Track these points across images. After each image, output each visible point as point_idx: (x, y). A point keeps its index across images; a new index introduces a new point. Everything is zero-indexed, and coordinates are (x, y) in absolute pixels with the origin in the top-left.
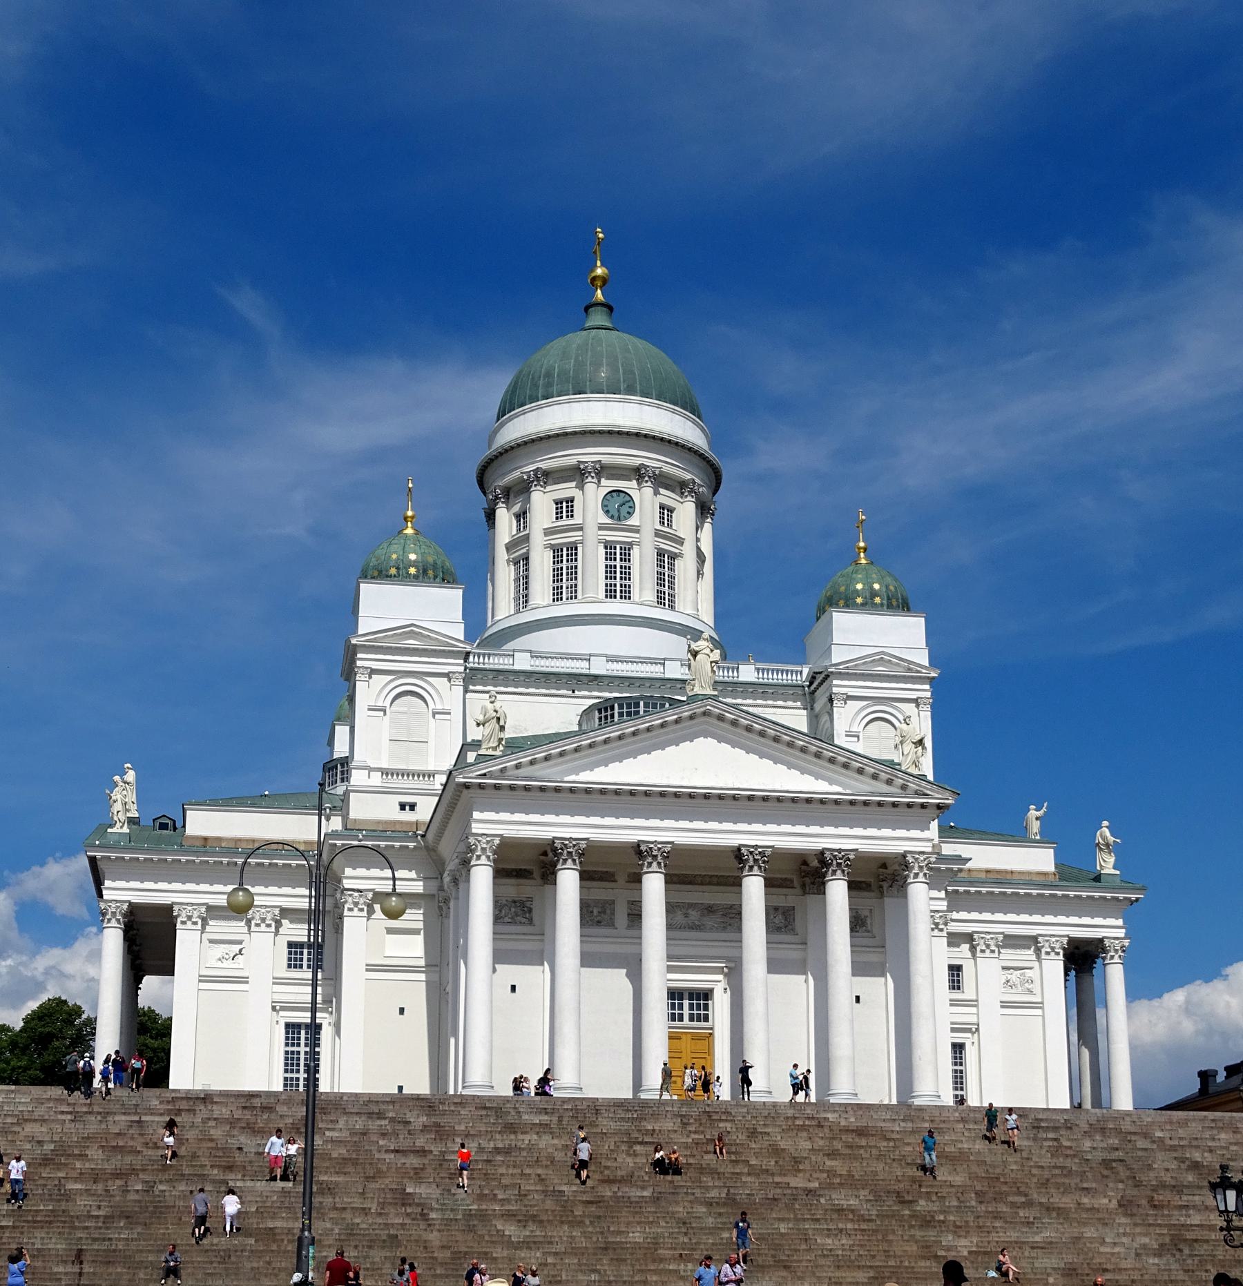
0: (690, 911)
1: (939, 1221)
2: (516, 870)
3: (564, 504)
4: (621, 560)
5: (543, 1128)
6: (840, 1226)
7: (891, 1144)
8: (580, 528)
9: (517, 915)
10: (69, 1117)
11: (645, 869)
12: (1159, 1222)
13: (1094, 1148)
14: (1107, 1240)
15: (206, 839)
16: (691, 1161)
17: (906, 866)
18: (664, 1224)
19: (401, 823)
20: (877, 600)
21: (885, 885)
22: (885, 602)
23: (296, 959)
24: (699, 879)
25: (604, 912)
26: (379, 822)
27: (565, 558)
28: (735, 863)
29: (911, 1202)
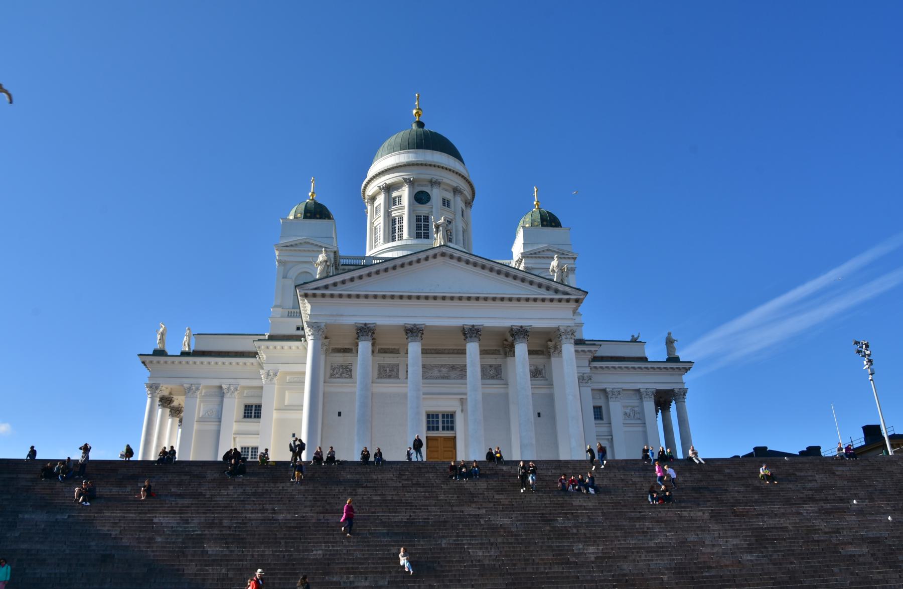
0: (442, 369)
1: (573, 534)
2: (343, 349)
4: (424, 221)
6: (492, 540)
7: (544, 483)
9: (343, 373)
12: (744, 527)
13: (686, 481)
14: (707, 543)
16: (395, 498)
17: (561, 335)
20: (545, 223)
21: (552, 350)
22: (549, 223)
23: (248, 413)
24: (446, 351)
25: (393, 370)
28: (463, 337)
29: (551, 520)
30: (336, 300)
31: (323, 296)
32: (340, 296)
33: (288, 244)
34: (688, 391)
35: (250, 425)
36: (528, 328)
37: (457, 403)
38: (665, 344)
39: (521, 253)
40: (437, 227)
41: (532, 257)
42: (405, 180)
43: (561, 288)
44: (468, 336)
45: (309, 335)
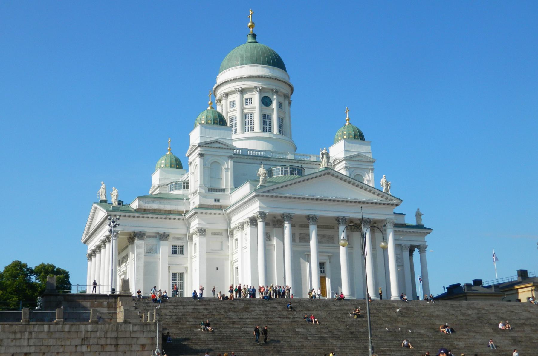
3: (249, 100)
4: (268, 119)
5: (316, 309)
7: (418, 313)
8: (254, 108)
10: (172, 307)
11: (311, 223)
15: (145, 209)
18: (376, 340)
19: (216, 205)
26: (208, 205)
27: (249, 117)
28: (336, 222)
30: (274, 199)
31: (267, 196)
32: (276, 197)
33: (205, 143)
34: (428, 247)
35: (178, 258)
36: (372, 219)
37: (327, 258)
38: (415, 215)
39: (344, 157)
40: (323, 154)
41: (349, 160)
42: (256, 88)
43: (389, 197)
44: (341, 222)
45: (259, 219)
